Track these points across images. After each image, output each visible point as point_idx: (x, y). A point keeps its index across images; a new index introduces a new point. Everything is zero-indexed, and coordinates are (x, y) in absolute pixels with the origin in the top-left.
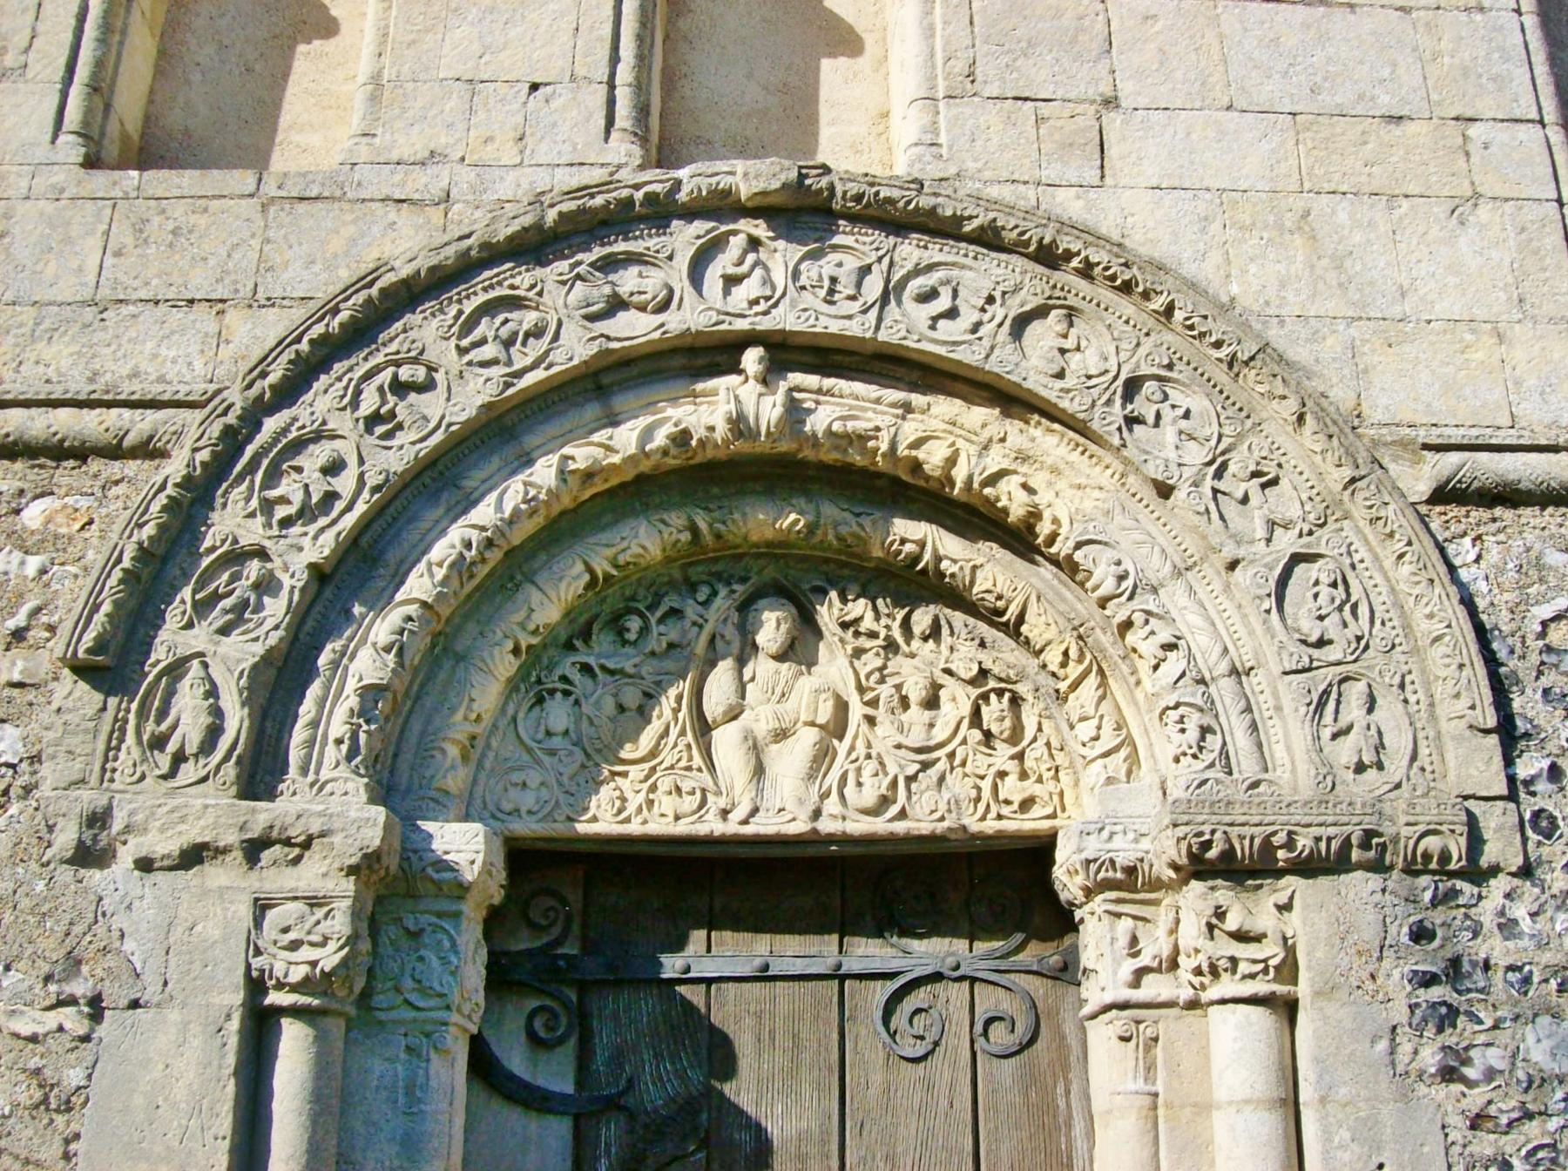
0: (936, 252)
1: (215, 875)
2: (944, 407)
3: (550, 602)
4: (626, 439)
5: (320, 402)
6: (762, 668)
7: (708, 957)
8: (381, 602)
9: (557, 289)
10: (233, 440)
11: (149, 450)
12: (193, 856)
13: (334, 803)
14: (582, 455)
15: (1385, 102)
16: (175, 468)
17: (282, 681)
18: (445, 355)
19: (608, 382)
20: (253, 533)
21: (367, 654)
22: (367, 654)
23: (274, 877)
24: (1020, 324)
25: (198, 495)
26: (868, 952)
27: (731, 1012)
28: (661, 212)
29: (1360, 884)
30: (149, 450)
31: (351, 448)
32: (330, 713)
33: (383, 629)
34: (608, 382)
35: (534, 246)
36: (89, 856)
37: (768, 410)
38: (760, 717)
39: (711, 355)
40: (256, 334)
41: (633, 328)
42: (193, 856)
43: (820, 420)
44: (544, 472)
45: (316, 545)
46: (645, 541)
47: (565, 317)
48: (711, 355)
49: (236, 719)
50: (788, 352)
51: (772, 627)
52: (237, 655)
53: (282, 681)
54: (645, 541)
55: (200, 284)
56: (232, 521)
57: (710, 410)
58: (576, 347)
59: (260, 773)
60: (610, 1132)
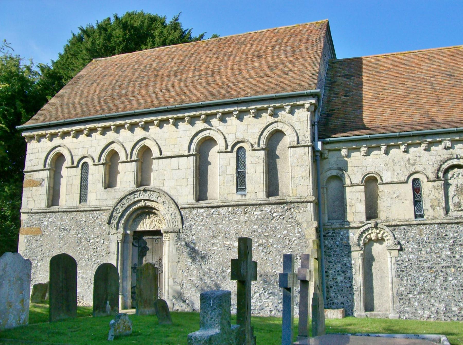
0: (153, 193)
1: (115, 235)
2: (154, 203)
3: (134, 216)
4: (136, 207)
5: (118, 206)
6: (147, 219)
7: (145, 238)
8: (123, 218)
9: (131, 197)
10: (114, 209)
11: (109, 210)
12: (114, 234)
13: (121, 230)
14: (134, 208)
15: (183, 178)
16: (111, 211)
17: (118, 223)
18: (125, 202)
19: (135, 203)
20: (116, 215)
21: (122, 221)
22: (122, 221)
23: (118, 235)
24: (158, 198)
25: (112, 213)
26: (154, 237)
27: (147, 241)
28: (137, 191)
29: (173, 233)
30: (109, 210)
31: (120, 209)
32: (121, 225)
33: (123, 220)
34: (135, 203)
35: (130, 194)
36: (109, 234)
37: (144, 204)
38: (146, 223)
39: (140, 201)
40: (115, 201)
41: (136, 199)
42: (114, 234)
43: (147, 205)
44: (132, 209)
45: (119, 215)
46: (139, 212)
47: (132, 199)
48: (140, 201)
49: (116, 226)
50: (145, 200)
51: (147, 217)
52: (116, 222)
53: (118, 223)
54: (139, 212)
55: (112, 198)
56: (114, 214)
57: (140, 204)
58: (132, 201)
59: (117, 229)
60: (140, 248)
